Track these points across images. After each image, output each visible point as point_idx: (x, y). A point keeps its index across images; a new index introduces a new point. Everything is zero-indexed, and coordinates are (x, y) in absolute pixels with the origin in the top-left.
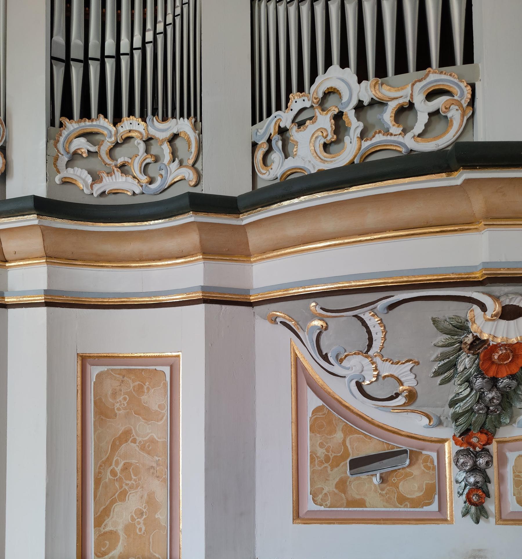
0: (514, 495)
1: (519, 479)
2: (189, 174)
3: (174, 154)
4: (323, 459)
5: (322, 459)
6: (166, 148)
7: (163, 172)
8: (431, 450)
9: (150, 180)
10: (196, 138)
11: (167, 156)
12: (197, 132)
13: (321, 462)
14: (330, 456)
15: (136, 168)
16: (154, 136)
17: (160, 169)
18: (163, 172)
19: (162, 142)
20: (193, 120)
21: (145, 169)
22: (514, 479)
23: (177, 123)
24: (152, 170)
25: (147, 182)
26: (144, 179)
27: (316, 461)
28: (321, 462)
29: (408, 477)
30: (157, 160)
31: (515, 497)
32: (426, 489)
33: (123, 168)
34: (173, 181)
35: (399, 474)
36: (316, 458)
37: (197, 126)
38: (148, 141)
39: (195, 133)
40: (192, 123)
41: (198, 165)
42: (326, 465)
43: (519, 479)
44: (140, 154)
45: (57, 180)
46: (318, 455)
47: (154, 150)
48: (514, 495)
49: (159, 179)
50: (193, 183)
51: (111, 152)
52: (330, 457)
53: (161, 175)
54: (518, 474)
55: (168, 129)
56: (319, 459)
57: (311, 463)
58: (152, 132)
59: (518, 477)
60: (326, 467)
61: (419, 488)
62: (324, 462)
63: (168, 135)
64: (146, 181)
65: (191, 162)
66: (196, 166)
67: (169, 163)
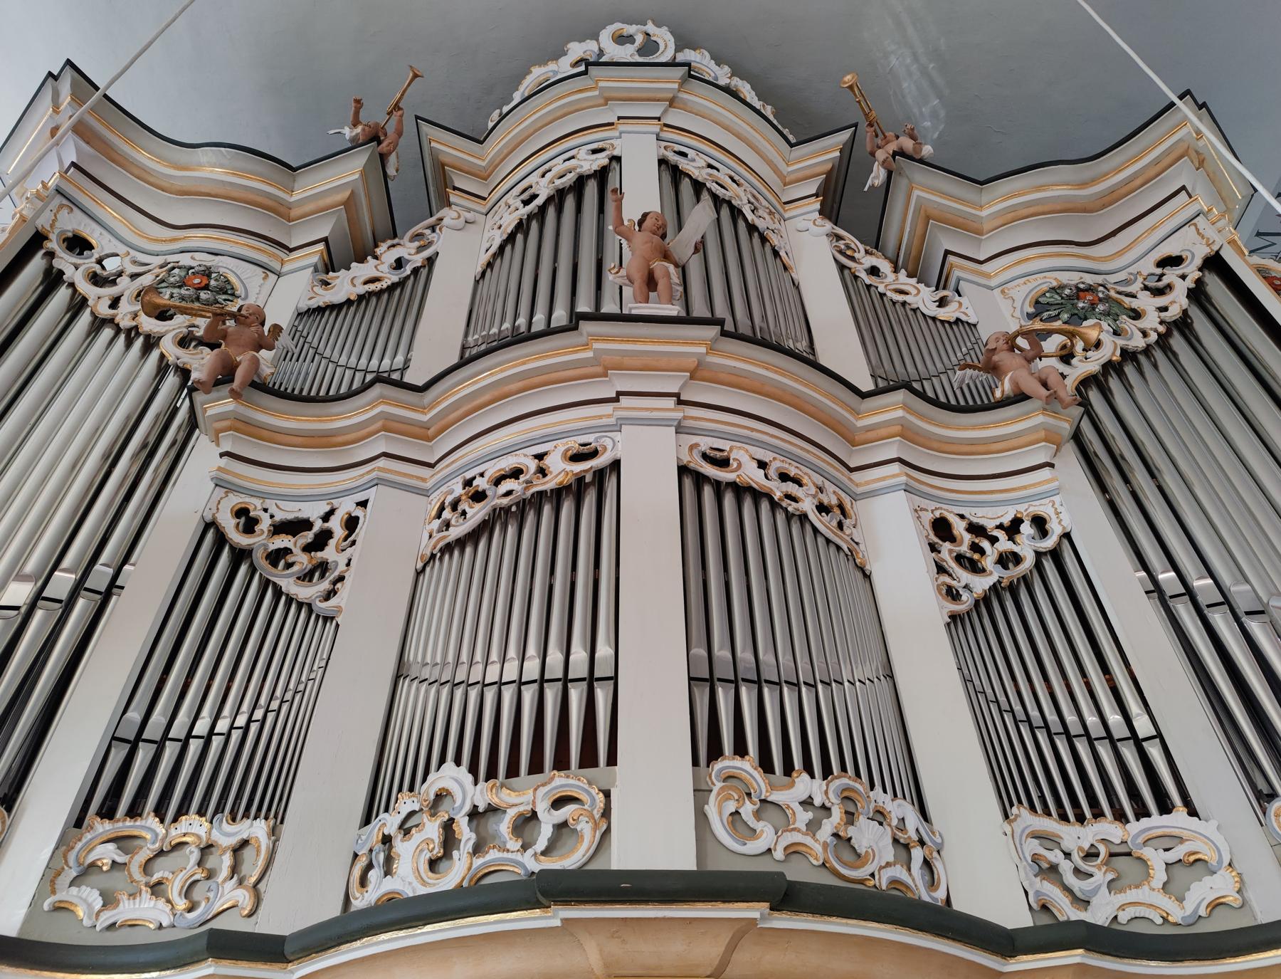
2: (243, 897)
3: (234, 869)
6: (227, 860)
7: (211, 895)
9: (191, 905)
10: (268, 847)
11: (225, 871)
12: (273, 838)
15: (174, 890)
16: (216, 842)
17: (209, 890)
18: (211, 895)
19: (224, 852)
20: (272, 822)
21: (188, 892)
23: (252, 825)
24: (197, 894)
25: (184, 909)
26: (181, 904)
30: (210, 875)
33: (157, 889)
34: (221, 909)
37: (274, 832)
38: (207, 849)
39: (269, 839)
40: (269, 826)
41: (261, 886)
44: (188, 868)
45: (46, 906)
47: (211, 862)
49: (203, 904)
50: (246, 912)
51: (147, 867)
53: (208, 899)
55: (237, 833)
58: (216, 836)
63: (234, 841)
64: (184, 907)
65: (253, 880)
66: (259, 886)
67: (224, 881)
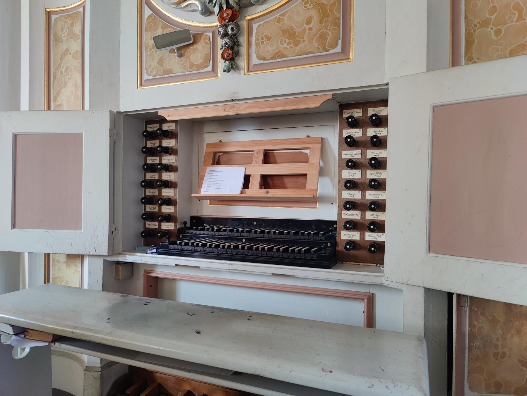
0: (255, 53)
1: (258, 41)
8: (209, 32)
22: (255, 42)
31: (255, 54)
32: (205, 58)
43: (258, 41)
48: (255, 53)
54: (258, 38)
59: (258, 40)
61: (201, 57)
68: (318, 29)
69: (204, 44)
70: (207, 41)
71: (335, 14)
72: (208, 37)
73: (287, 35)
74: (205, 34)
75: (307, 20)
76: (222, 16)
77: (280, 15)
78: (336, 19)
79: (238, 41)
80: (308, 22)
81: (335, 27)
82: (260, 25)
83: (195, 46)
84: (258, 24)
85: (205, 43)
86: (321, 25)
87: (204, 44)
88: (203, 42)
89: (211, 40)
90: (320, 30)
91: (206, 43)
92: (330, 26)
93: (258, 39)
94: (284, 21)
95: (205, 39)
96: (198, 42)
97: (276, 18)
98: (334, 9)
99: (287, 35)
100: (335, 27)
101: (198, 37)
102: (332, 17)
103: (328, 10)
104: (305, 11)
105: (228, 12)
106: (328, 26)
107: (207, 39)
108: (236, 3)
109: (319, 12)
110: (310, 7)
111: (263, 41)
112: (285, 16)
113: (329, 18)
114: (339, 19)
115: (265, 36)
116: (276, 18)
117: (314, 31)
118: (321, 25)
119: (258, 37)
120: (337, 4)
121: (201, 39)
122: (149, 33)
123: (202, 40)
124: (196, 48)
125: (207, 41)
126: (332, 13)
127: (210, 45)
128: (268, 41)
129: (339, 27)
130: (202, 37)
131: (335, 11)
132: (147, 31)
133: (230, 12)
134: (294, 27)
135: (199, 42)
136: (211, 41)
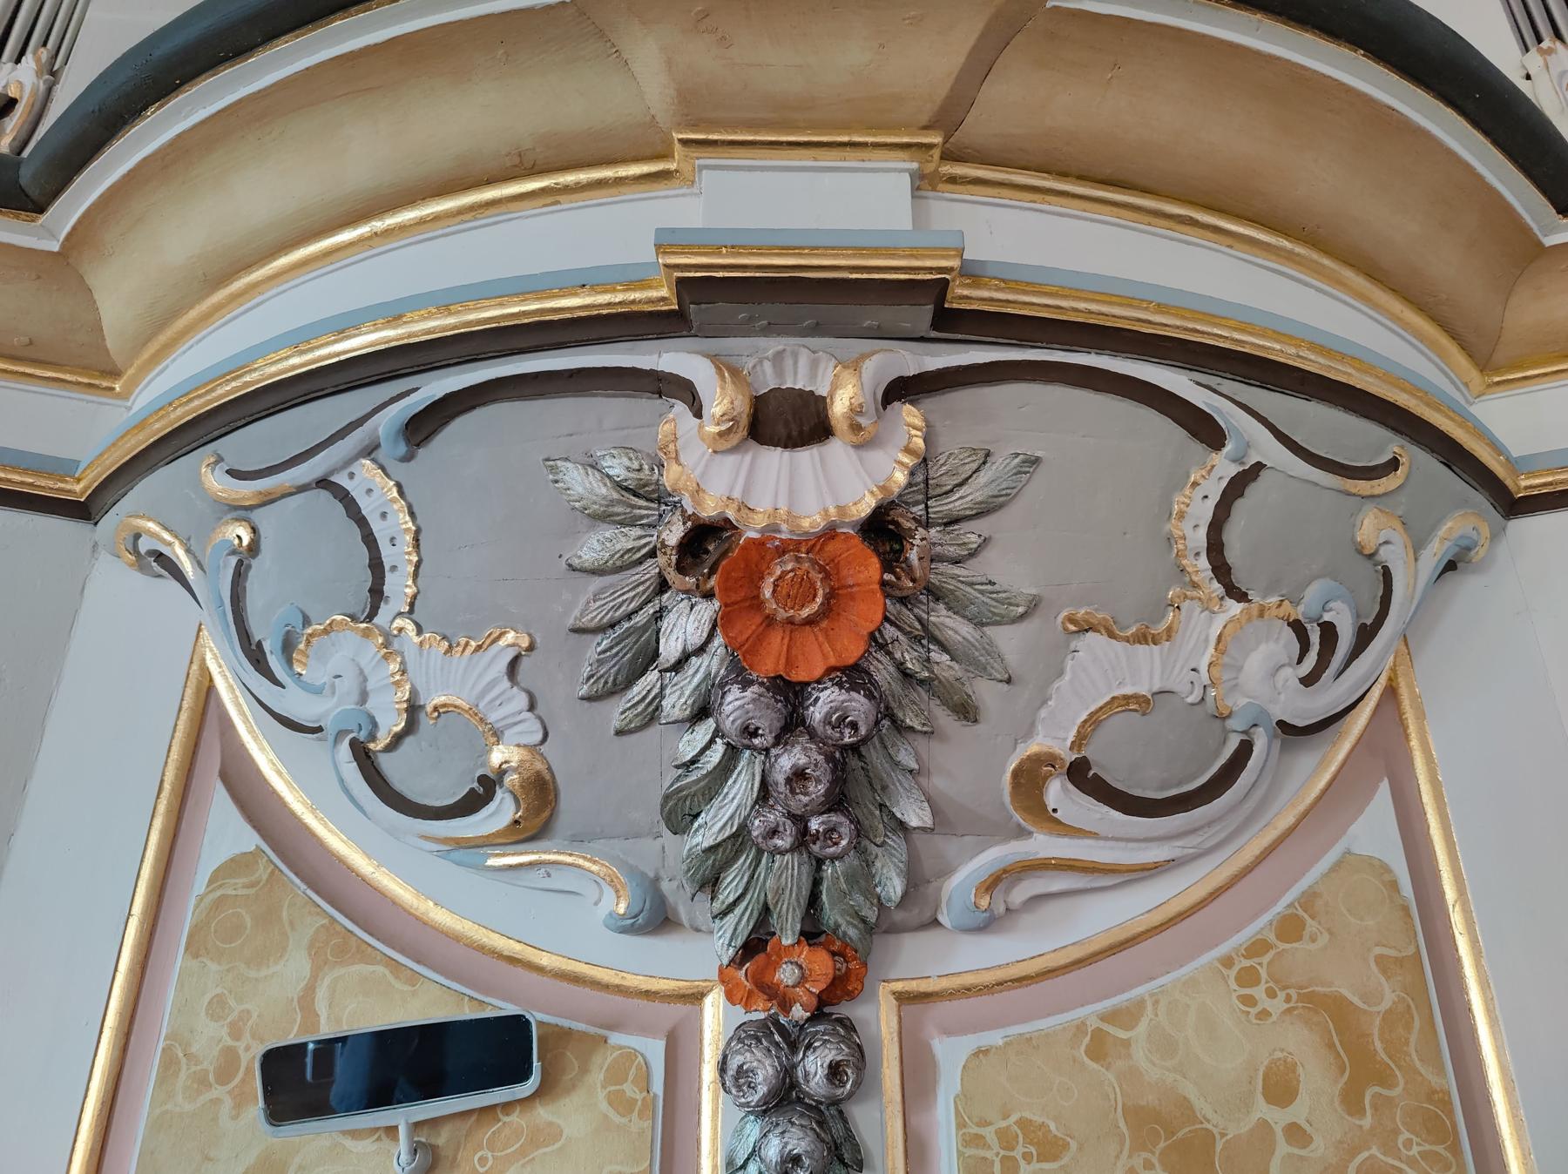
4: (211, 1069)
5: (205, 1065)
13: (202, 1082)
14: (241, 1052)
27: (183, 1075)
28: (202, 1082)
29: (538, 1148)
35: (507, 1131)
36: (184, 1060)
42: (218, 1091)
46: (194, 1049)
52: (239, 1057)
56: (193, 1069)
57: (162, 1080)
60: (216, 1102)
62: (211, 1078)
68: (1341, 1142)
69: (604, 1106)
70: (629, 1093)
71: (1421, 1075)
72: (639, 1068)
73: (1162, 1145)
74: (616, 1038)
75: (1266, 1077)
76: (767, 979)
77: (1104, 1018)
78: (1429, 1099)
79: (850, 1136)
80: (1281, 1088)
81: (1434, 1148)
82: (981, 1053)
83: (543, 1113)
84: (968, 1043)
85: (610, 1104)
86: (1358, 1122)
87: (612, 1114)
88: (601, 1095)
89: (658, 1087)
90: (1354, 1152)
91: (622, 1105)
92: (1407, 1135)
93: (977, 1141)
94: (1129, 1056)
95: (616, 1075)
96: (569, 1090)
97: (1078, 1027)
98: (1407, 1040)
99: (1162, 1145)
100: (1434, 1148)
101: (569, 1054)
102: (1406, 1083)
103: (1378, 1045)
104: (1249, 1021)
105: (801, 961)
106: (1396, 1132)
107: (631, 1077)
108: (864, 920)
109: (1331, 1046)
110: (1277, 1006)
111: (1014, 1159)
112: (1131, 1028)
113: (1391, 1087)
114: (1446, 1104)
115: (1023, 1123)
116: (1081, 1027)
117: (1320, 1147)
118: (1358, 1122)
119: (979, 1125)
120: (1416, 1017)
121: (584, 1070)
122: (213, 966)
123: (597, 1076)
124: (551, 1124)
125: (630, 1090)
126: (1403, 1063)
127: (647, 1124)
128: (1046, 1166)
129: (1456, 1149)
130: (597, 1059)
131: (1414, 1056)
132: (196, 956)
133: (821, 965)
134: (1201, 1106)
135: (574, 1086)
136: (655, 1096)
